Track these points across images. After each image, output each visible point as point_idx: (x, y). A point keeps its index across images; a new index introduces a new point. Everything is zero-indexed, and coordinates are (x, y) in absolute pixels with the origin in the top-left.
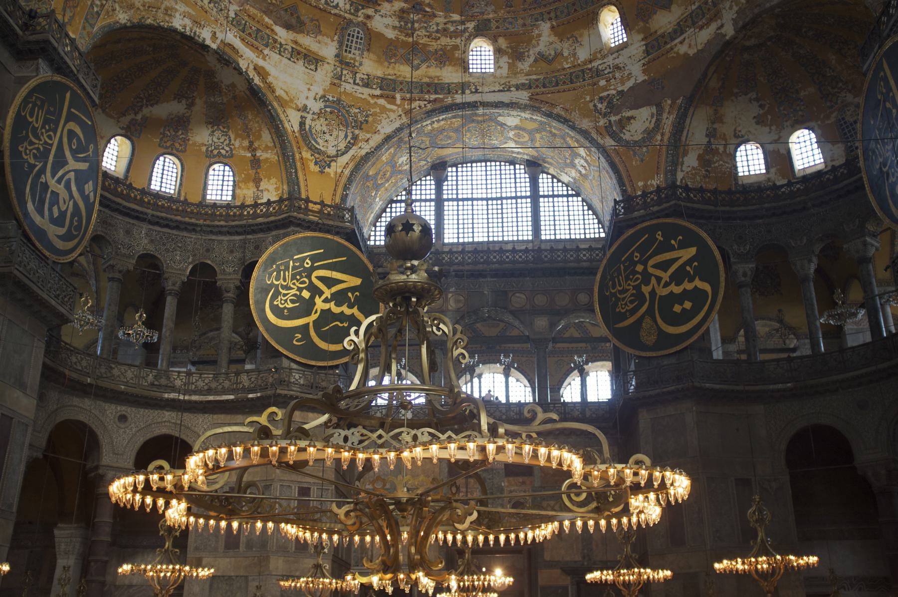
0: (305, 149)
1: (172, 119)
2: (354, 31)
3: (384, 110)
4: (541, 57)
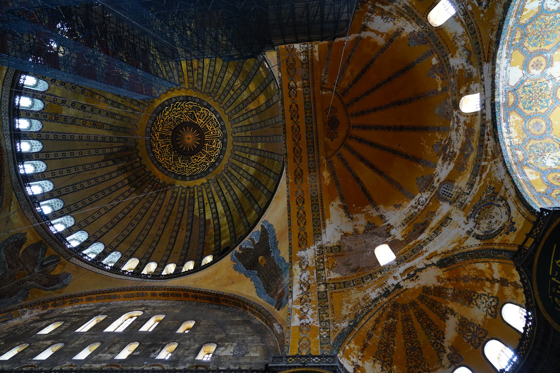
0: (495, 239)
1: (460, 329)
2: (442, 190)
3: (489, 175)
4: (468, 60)
